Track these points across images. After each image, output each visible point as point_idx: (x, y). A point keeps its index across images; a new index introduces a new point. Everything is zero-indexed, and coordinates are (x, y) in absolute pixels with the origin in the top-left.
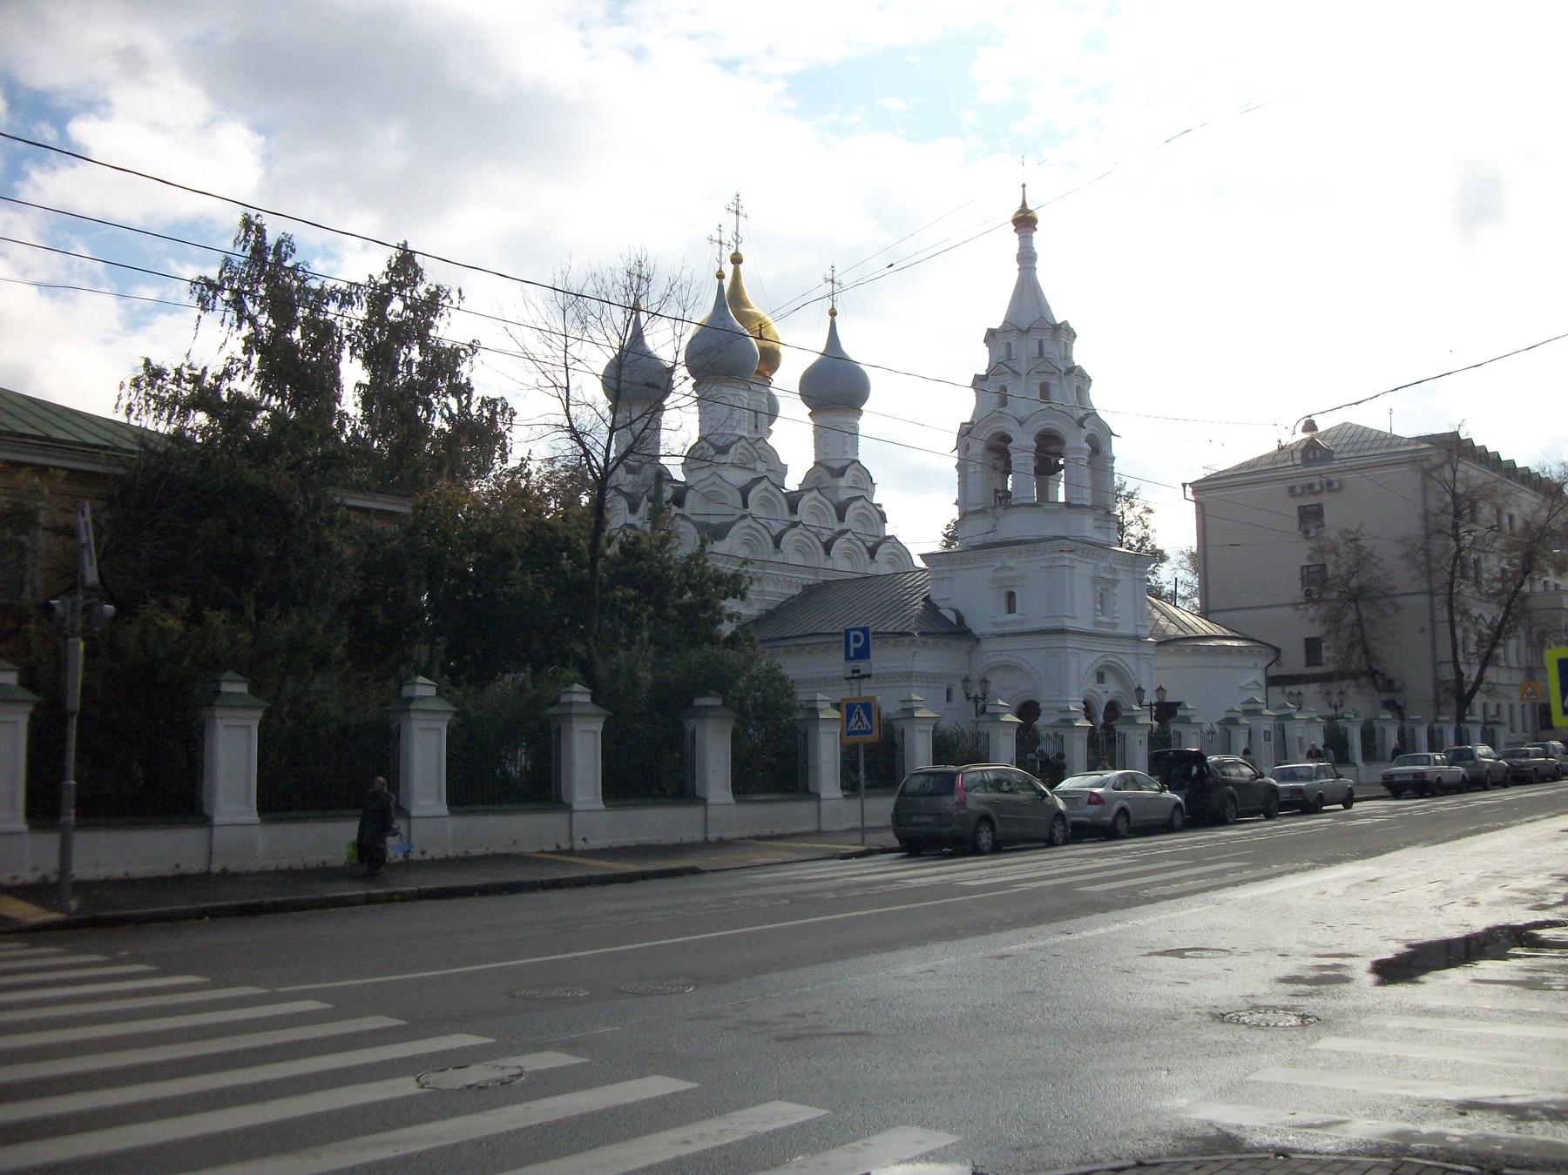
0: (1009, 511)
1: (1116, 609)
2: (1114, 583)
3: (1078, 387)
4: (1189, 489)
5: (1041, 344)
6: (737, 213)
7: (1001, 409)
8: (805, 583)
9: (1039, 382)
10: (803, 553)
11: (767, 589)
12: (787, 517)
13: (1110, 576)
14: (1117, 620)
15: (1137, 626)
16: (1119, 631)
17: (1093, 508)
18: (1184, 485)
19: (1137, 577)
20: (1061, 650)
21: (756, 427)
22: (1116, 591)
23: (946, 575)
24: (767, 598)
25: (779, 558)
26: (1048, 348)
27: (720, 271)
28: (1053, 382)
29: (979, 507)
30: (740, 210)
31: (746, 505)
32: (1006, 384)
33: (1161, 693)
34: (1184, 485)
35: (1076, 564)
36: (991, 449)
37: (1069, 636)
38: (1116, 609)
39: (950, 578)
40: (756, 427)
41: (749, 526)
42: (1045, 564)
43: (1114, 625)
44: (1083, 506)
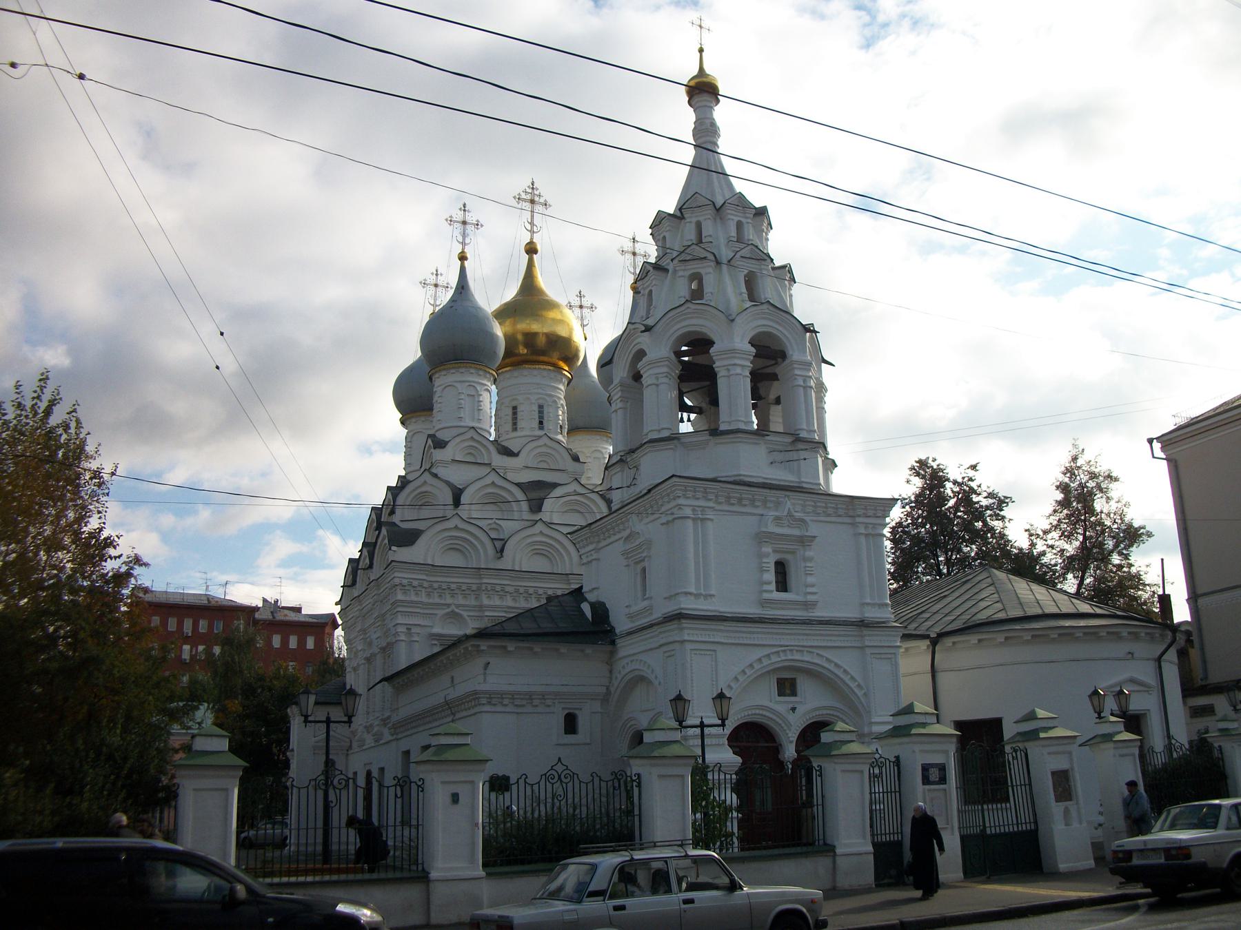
1: (810, 580)
2: (805, 541)
4: (1157, 446)
5: (699, 226)
6: (532, 202)
8: (550, 592)
9: (687, 273)
10: (548, 557)
11: (486, 602)
12: (527, 515)
13: (796, 532)
14: (810, 598)
15: (863, 604)
16: (819, 613)
18: (1150, 441)
19: (862, 531)
20: (677, 646)
21: (541, 423)
22: (809, 554)
24: (487, 614)
25: (506, 563)
27: (463, 252)
28: (708, 271)
30: (537, 199)
31: (457, 502)
33: (680, 704)
34: (1150, 441)
37: (685, 623)
38: (810, 580)
39: (598, 560)
40: (541, 423)
41: (456, 527)
42: (664, 519)
43: (807, 605)
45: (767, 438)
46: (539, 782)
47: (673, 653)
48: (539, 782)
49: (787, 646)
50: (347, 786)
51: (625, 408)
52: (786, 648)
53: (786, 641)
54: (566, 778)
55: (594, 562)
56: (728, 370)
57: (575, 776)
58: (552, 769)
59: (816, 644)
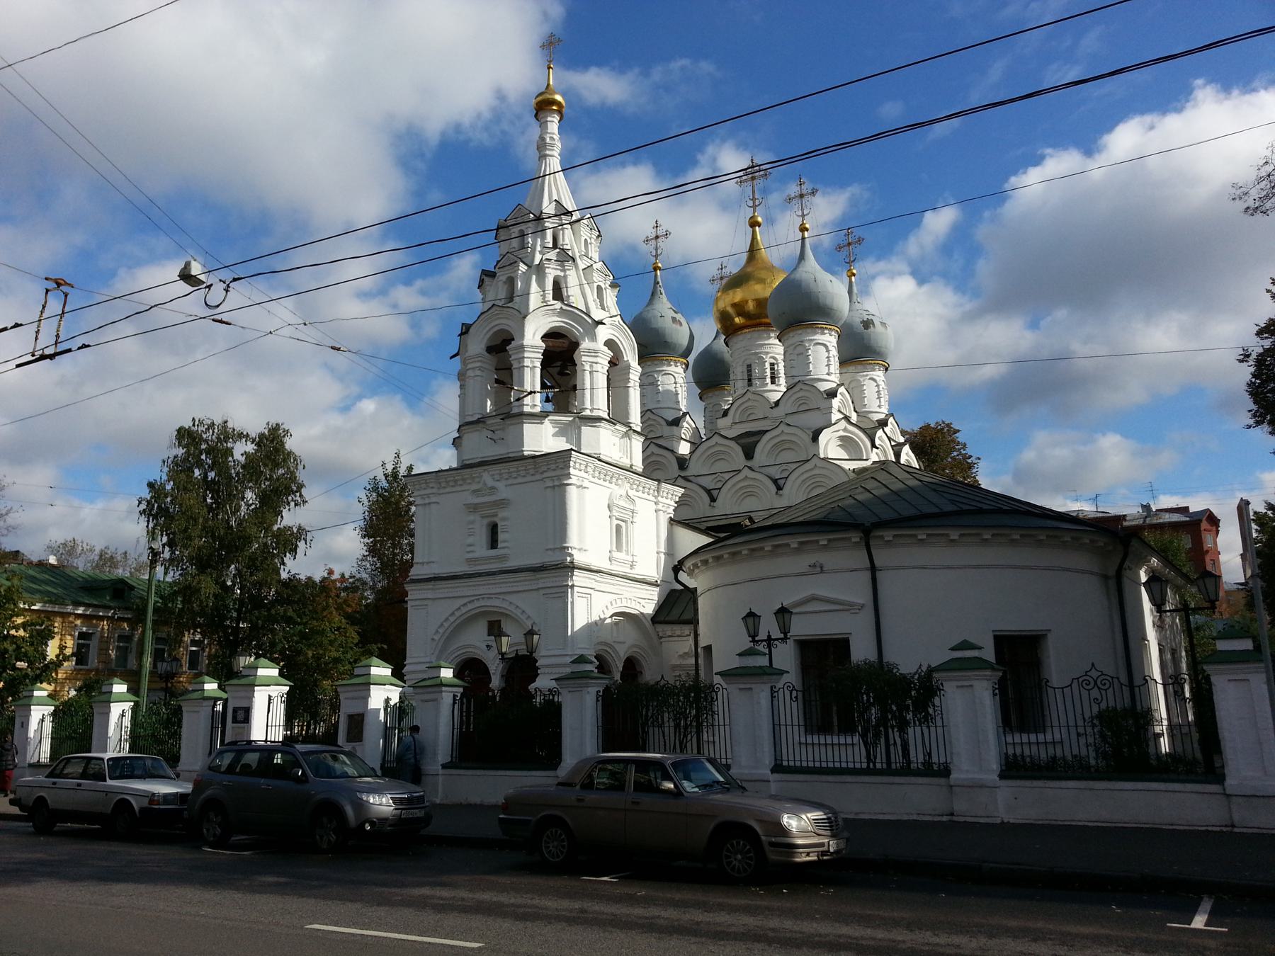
0: (508, 422)
3: (599, 287)
7: (509, 305)
17: (612, 421)
23: (433, 499)
26: (567, 238)
29: (475, 418)
32: (512, 275)
35: (586, 484)
36: (490, 350)
39: (438, 503)
44: (600, 419)
45: (616, 427)
46: (1071, 685)
47: (563, 594)
48: (1071, 685)
49: (480, 595)
50: (1112, 684)
51: (482, 376)
52: (479, 597)
53: (481, 590)
54: (1105, 684)
55: (433, 506)
56: (591, 366)
57: (1115, 680)
58: (1086, 675)
59: (498, 590)
